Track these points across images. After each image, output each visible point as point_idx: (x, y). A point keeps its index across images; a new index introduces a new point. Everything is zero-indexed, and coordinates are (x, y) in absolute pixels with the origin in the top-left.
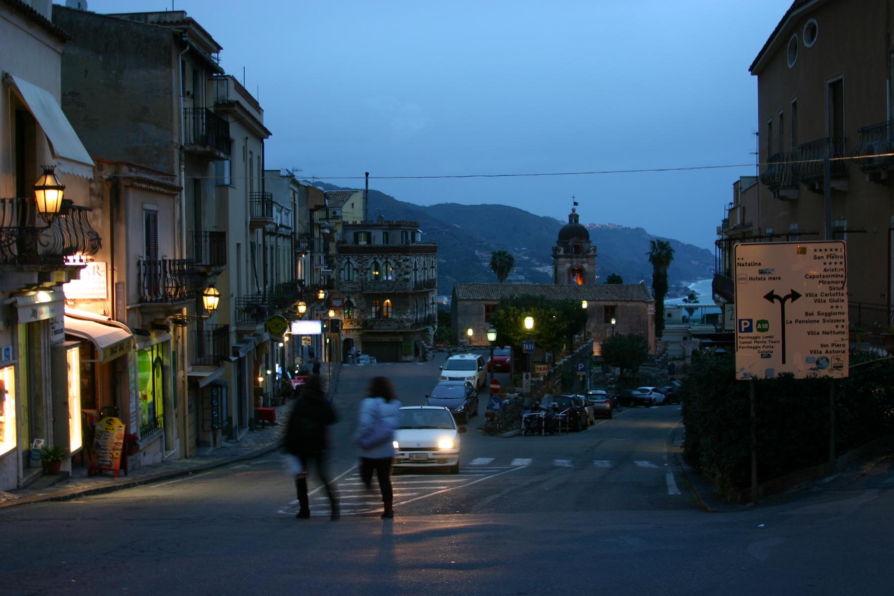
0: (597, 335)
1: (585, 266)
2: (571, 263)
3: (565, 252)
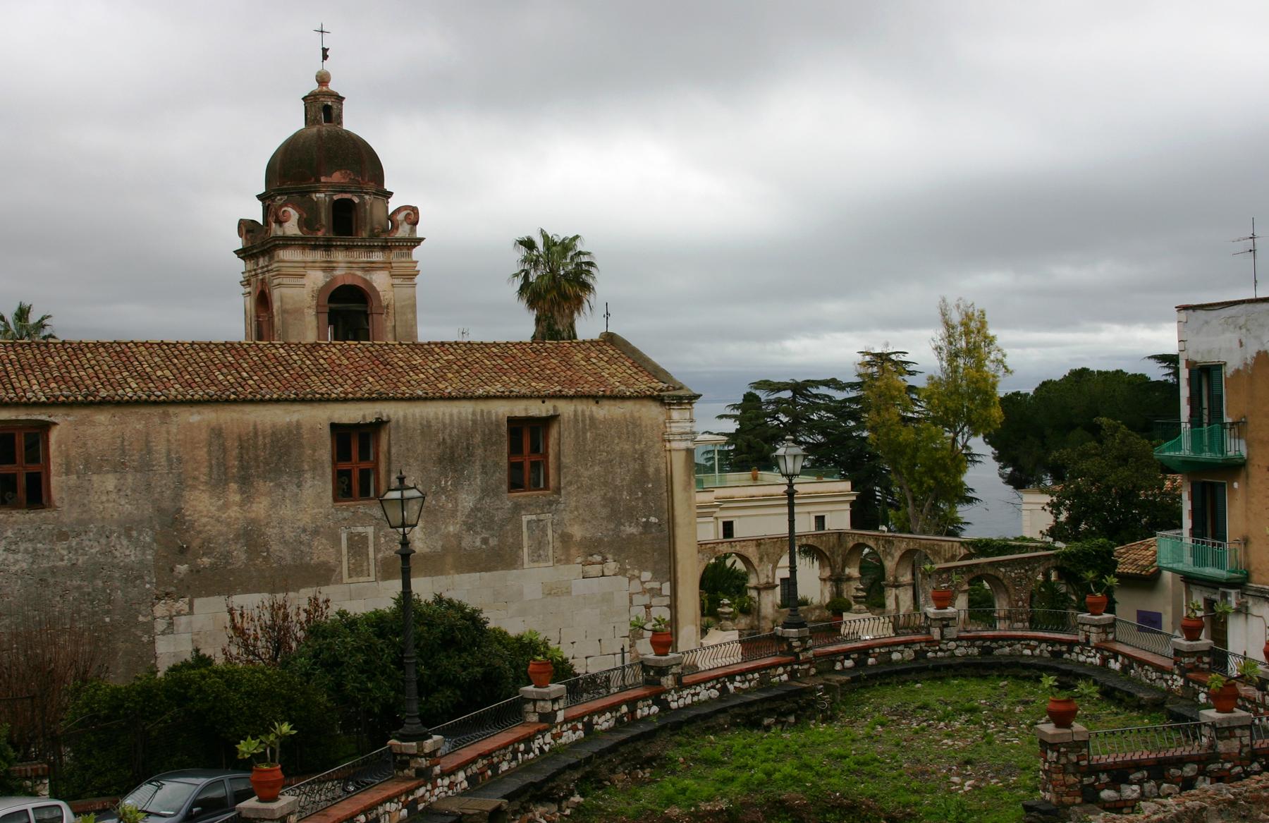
0: (485, 541)
1: (380, 281)
2: (329, 268)
3: (302, 223)
